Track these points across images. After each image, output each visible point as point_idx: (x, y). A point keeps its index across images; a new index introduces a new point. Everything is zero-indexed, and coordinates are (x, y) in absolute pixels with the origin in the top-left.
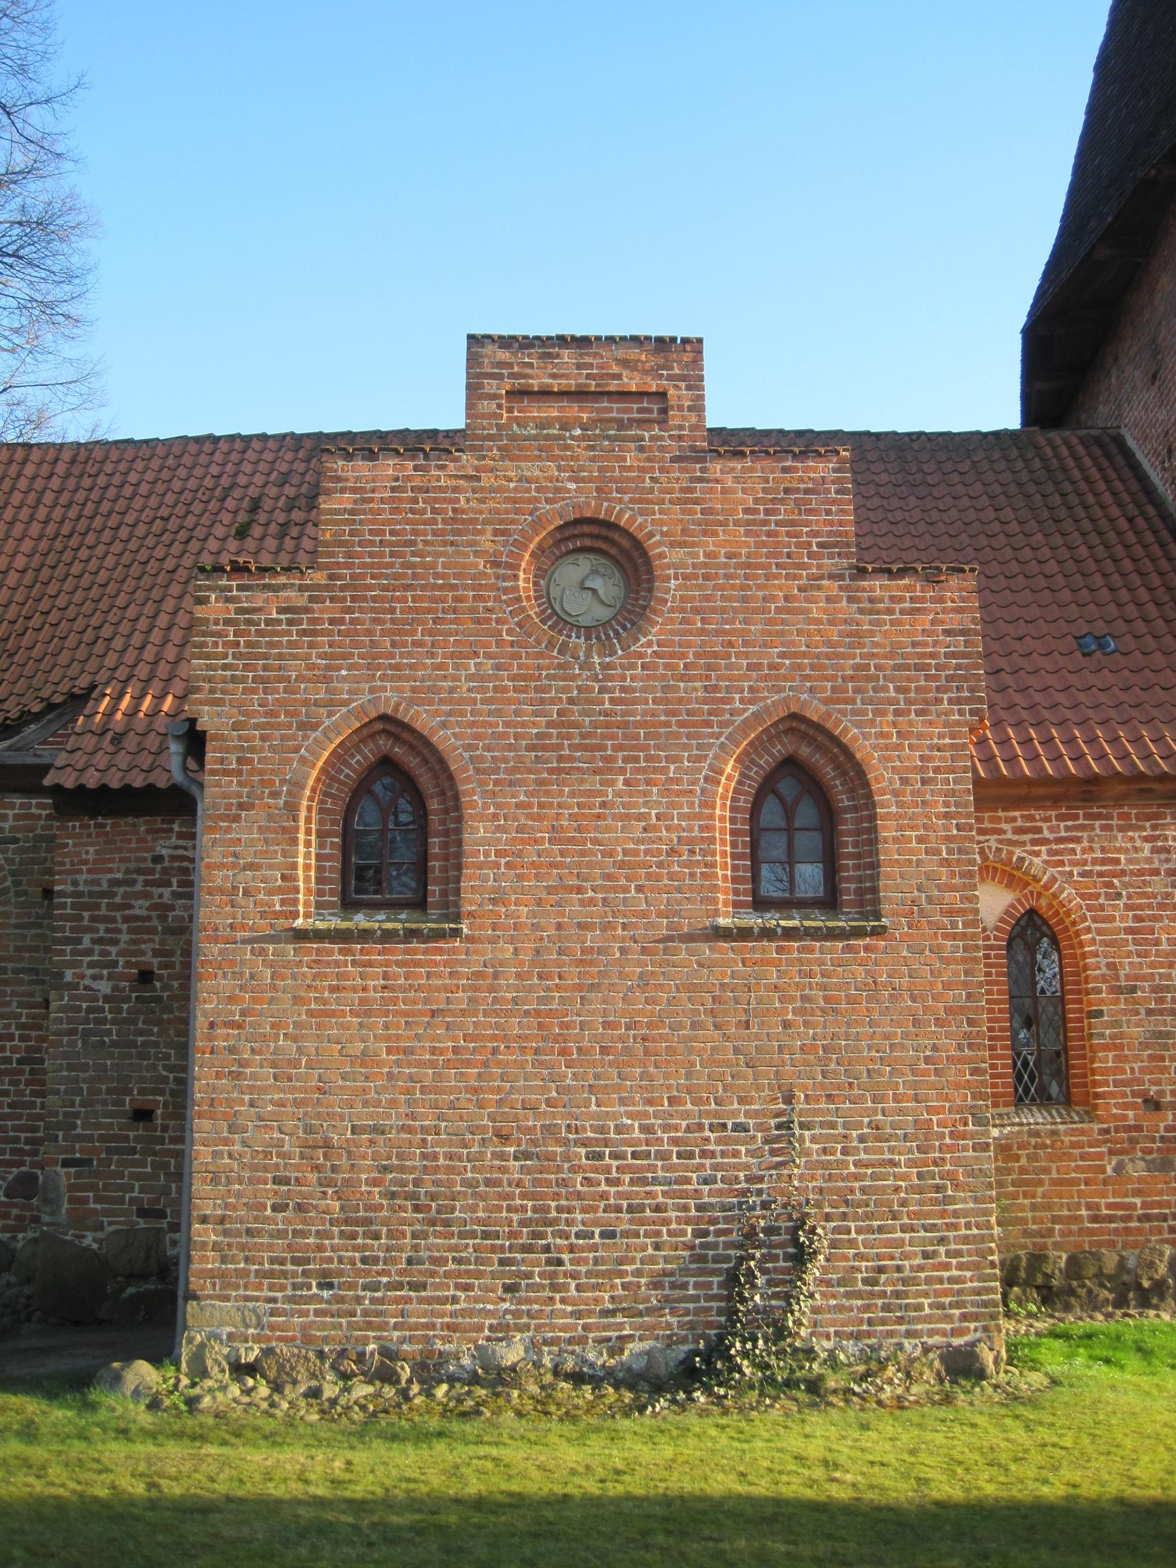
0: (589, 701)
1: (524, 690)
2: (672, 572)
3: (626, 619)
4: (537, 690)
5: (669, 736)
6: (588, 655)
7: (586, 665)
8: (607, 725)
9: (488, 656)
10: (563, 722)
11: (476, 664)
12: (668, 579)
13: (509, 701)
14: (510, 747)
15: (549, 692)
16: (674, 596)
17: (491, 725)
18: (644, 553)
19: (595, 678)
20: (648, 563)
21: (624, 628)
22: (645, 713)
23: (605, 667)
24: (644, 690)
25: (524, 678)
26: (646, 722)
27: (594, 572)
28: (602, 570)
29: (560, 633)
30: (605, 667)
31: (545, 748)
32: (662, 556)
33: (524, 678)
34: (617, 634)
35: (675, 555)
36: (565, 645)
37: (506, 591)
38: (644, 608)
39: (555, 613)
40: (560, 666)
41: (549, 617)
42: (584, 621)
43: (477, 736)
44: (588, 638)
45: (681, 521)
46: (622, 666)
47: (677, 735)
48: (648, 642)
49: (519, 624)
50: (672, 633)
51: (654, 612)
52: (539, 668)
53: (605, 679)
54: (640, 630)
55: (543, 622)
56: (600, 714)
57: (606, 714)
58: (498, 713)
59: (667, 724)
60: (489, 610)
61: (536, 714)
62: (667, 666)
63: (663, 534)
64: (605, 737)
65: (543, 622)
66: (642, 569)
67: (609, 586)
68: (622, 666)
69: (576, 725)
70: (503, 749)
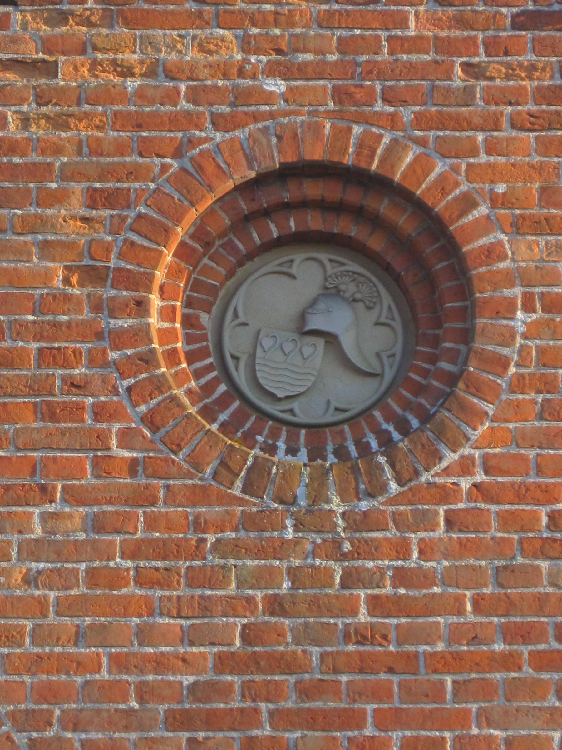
0: (317, 606)
1: (162, 580)
2: (517, 291)
3: (406, 405)
4: (195, 579)
5: (513, 690)
6: (317, 495)
7: (313, 519)
8: (364, 665)
9: (74, 497)
10: (256, 658)
11: (45, 517)
12: (509, 309)
13: (126, 607)
14: (129, 720)
15: (224, 584)
16: (523, 350)
17: (80, 665)
18: (450, 247)
19: (334, 550)
20: (459, 267)
21: (404, 428)
22: (456, 634)
23: (359, 522)
24: (449, 579)
25: (162, 550)
26: (458, 657)
27: (331, 292)
28: (350, 288)
29: (248, 439)
30: (359, 522)
31: (212, 721)
32: (493, 253)
33: (162, 550)
34: (386, 442)
35: (521, 252)
36: (259, 470)
37: (119, 339)
38: (452, 380)
39: (235, 390)
40: (249, 522)
41: (223, 402)
42: (307, 412)
43: (48, 694)
44: (316, 453)
45: (539, 169)
46: (400, 521)
47: (536, 689)
48: (463, 461)
49: (150, 420)
50: (521, 438)
51: (477, 389)
52: (199, 525)
53: (358, 553)
54: (441, 433)
55: (209, 413)
56: (347, 638)
57: (362, 636)
58: (100, 635)
59: (509, 662)
60: (75, 386)
61: (191, 637)
62: (507, 521)
63: (495, 201)
64: (358, 693)
65: (209, 413)
66: (446, 285)
67: (365, 328)
68: (400, 521)
69: (285, 664)
70: (111, 724)
